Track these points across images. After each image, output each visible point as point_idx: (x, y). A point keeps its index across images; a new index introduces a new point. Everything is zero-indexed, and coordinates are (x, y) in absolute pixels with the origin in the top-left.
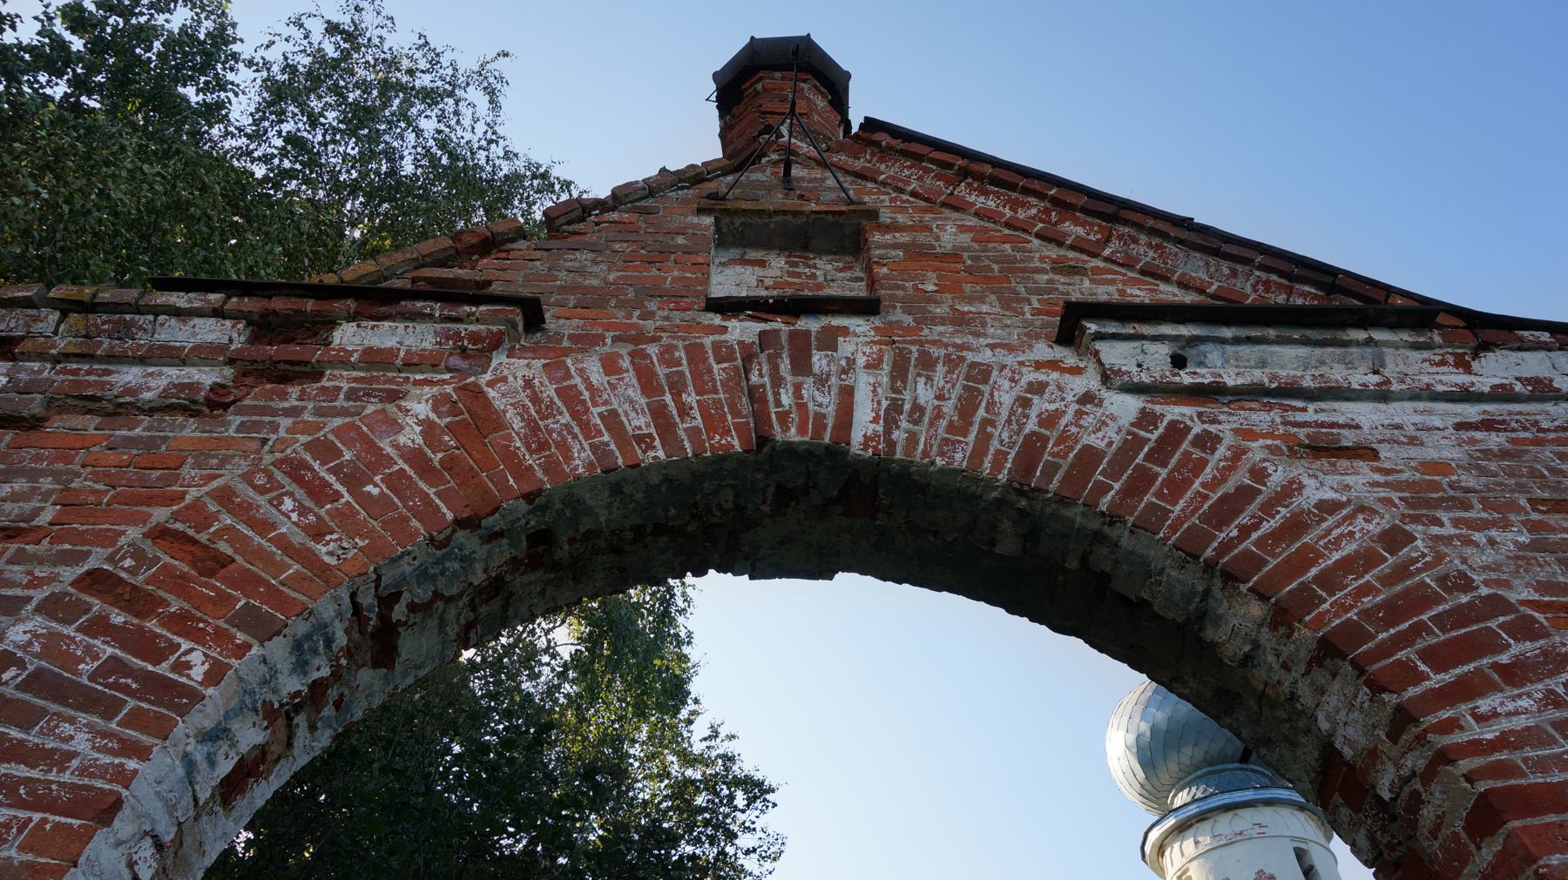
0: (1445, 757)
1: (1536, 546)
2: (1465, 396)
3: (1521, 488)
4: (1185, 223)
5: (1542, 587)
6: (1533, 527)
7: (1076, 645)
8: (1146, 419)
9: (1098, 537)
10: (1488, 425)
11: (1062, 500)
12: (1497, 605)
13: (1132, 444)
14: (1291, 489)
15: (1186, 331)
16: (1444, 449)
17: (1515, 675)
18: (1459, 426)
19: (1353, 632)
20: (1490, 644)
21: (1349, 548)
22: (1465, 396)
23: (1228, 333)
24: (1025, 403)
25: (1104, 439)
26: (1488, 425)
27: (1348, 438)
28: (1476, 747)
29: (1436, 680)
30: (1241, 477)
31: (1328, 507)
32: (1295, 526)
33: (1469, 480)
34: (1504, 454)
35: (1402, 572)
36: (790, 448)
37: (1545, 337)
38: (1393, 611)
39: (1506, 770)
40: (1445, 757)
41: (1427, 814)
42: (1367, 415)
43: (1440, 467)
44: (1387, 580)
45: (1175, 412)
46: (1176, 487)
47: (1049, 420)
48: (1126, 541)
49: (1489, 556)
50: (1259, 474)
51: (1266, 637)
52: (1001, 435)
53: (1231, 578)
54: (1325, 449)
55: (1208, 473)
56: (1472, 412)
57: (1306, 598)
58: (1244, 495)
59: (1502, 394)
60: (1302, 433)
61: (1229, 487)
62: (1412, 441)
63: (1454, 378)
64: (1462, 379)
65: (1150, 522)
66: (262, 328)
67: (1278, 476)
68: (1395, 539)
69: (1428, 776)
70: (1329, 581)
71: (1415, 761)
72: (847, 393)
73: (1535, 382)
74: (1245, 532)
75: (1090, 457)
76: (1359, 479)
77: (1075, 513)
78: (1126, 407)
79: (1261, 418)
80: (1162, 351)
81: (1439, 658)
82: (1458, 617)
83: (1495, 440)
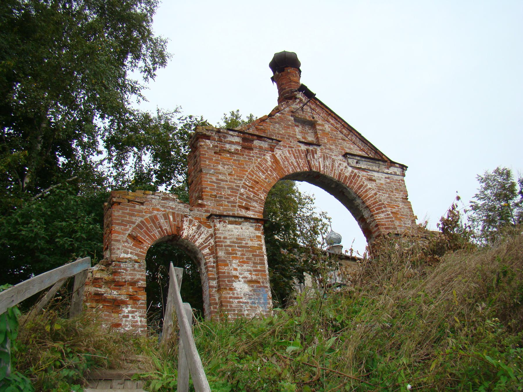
0: (375, 220)
1: (389, 197)
2: (387, 173)
3: (389, 189)
4: (359, 134)
5: (388, 202)
6: (389, 194)
7: (333, 197)
8: (352, 172)
9: (345, 188)
10: (388, 178)
11: (343, 183)
12: (383, 204)
13: (351, 176)
14: (367, 185)
15: (359, 158)
16: (383, 182)
17: (383, 212)
18: (386, 178)
19: (370, 205)
20: (381, 208)
21: (371, 195)
22: (387, 173)
23: (363, 159)
24: (339, 167)
25: (347, 174)
26: (388, 178)
27: (374, 178)
28: (378, 219)
29: (376, 212)
30: (362, 183)
31: (370, 189)
32: (366, 191)
33: (384, 187)
34: (389, 183)
35: (375, 199)
36: (314, 171)
37: (398, 166)
38: (374, 203)
39: (380, 222)
40: (375, 220)
41: (371, 225)
42: (375, 174)
43: (382, 184)
44: (374, 199)
45: (356, 171)
46: (355, 183)
47: (342, 170)
48: (349, 189)
49: (383, 198)
50: (364, 183)
51: (361, 204)
52: (337, 172)
53: (359, 197)
54: (371, 180)
55: (358, 182)
56: (387, 176)
57: (366, 201)
58: (362, 185)
59: (391, 174)
60: (369, 176)
61: (360, 184)
62: (380, 180)
63: (386, 171)
64: (387, 171)
65: (351, 189)
66: (244, 140)
67: (365, 184)
68: (376, 194)
69: (373, 221)
70: (368, 199)
71: (372, 220)
72: (319, 162)
73: (395, 172)
74: (362, 191)
75: (346, 177)
76: (374, 184)
77: (344, 185)
78: (350, 169)
79: (365, 173)
80: (355, 161)
81: (377, 209)
82: (379, 205)
83: (388, 181)
